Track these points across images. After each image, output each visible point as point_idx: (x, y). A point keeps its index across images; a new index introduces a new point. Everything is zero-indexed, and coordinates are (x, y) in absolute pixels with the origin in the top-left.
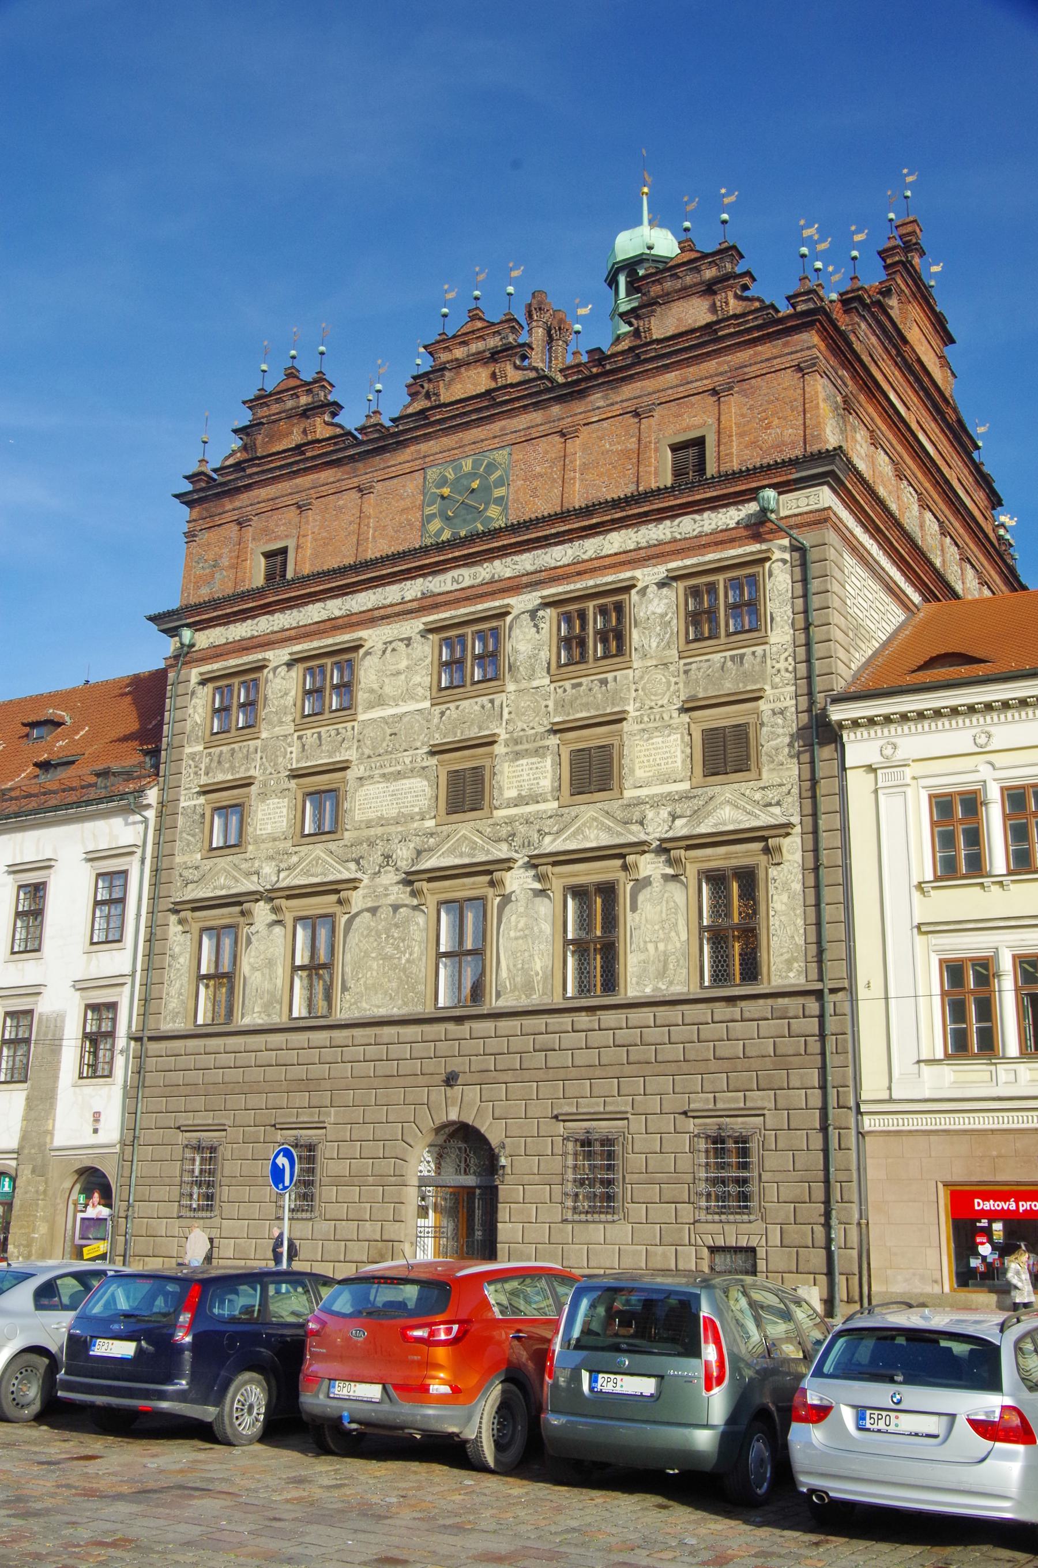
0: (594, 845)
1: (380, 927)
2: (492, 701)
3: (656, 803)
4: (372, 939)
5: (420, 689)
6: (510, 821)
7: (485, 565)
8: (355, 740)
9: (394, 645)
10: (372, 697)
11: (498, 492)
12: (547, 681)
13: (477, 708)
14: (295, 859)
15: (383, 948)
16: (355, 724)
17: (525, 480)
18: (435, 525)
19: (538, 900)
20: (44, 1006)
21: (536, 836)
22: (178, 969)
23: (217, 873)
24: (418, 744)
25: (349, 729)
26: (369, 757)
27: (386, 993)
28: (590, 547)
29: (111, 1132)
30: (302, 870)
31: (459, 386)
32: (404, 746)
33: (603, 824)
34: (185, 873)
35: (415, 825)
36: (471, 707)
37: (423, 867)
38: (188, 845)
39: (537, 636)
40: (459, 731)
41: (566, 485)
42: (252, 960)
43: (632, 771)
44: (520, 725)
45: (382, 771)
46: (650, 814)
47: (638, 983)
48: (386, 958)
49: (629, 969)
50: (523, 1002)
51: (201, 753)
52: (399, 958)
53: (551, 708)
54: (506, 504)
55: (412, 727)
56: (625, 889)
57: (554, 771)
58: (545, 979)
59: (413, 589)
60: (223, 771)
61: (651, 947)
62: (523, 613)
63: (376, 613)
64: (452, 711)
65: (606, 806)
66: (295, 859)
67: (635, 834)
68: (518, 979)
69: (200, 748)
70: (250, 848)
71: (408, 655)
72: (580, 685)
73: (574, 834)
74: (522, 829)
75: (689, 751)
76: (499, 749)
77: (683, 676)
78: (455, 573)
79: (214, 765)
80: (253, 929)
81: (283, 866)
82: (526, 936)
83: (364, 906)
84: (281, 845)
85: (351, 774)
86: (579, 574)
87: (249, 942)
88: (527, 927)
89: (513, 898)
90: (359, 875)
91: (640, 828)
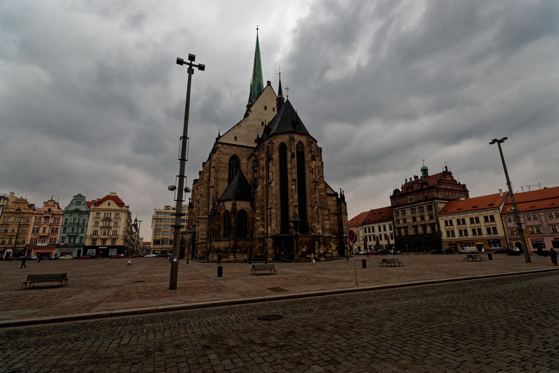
20: (388, 234)
28: (420, 204)
29: (394, 243)
36: (414, 214)
59: (408, 206)
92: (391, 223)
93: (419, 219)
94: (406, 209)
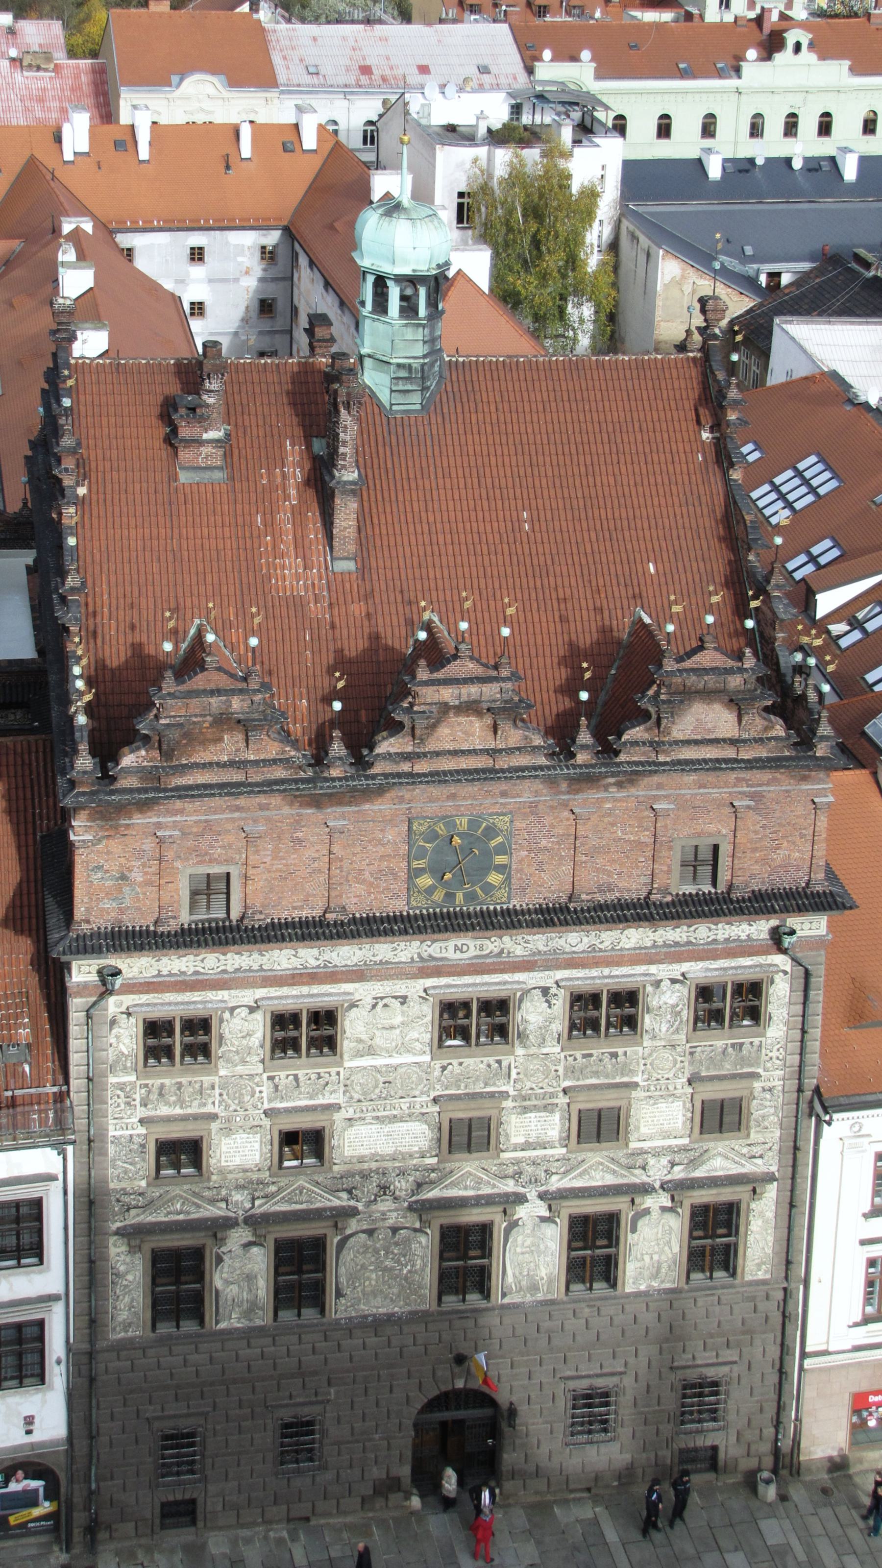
0: (600, 1183)
1: (378, 1245)
2: (499, 1062)
3: (657, 1153)
4: (369, 1255)
5: (417, 1043)
6: (517, 1162)
7: (493, 939)
8: (341, 1085)
9: (385, 1001)
10: (361, 1047)
11: (500, 859)
12: (558, 1049)
13: (483, 1066)
14: (273, 1188)
15: (382, 1262)
16: (341, 1070)
17: (529, 851)
18: (425, 881)
19: (544, 1225)
21: (543, 1174)
22: (126, 1286)
23: (171, 1200)
24: (417, 1093)
25: (333, 1073)
26: (359, 1101)
30: (283, 1198)
31: (447, 731)
32: (400, 1093)
33: (608, 1167)
34: (126, 1199)
35: (415, 1162)
39: (549, 1010)
40: (463, 1085)
41: (577, 868)
43: (638, 1128)
44: (529, 1085)
45: (375, 1114)
46: (652, 1161)
47: (634, 1283)
49: (628, 1273)
52: (401, 1270)
53: (561, 1072)
54: (509, 873)
55: (409, 1078)
56: (627, 1216)
57: (563, 1125)
58: (550, 1281)
61: (647, 1258)
62: (535, 988)
64: (455, 1068)
67: (638, 1177)
68: (524, 1283)
70: (214, 1178)
71: (403, 1013)
72: (591, 1055)
73: (580, 1175)
75: (689, 1115)
76: (508, 1104)
77: (688, 1057)
80: (224, 1249)
81: (257, 1194)
82: (532, 1251)
83: (359, 1228)
84: (255, 1177)
85: (339, 1117)
87: (219, 1260)
88: (533, 1244)
89: (520, 1223)
90: (352, 1203)
91: (641, 1171)
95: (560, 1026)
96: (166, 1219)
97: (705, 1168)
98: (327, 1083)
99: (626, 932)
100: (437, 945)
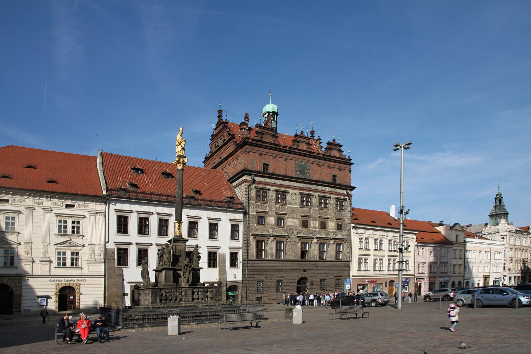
2: (309, 210)
3: (332, 232)
6: (312, 230)
10: (289, 202)
12: (317, 209)
13: (307, 210)
14: (276, 230)
19: (316, 244)
23: (260, 229)
27: (293, 256)
28: (324, 188)
32: (295, 213)
34: (253, 228)
36: (306, 209)
37: (299, 236)
38: (253, 222)
42: (268, 247)
43: (328, 226)
44: (313, 215)
46: (331, 234)
48: (293, 250)
50: (314, 259)
51: (254, 203)
59: (296, 184)
60: (259, 208)
63: (291, 187)
65: (325, 231)
66: (276, 230)
68: (313, 256)
69: (254, 202)
70: (267, 226)
71: (296, 197)
73: (321, 235)
74: (314, 232)
78: (304, 184)
79: (257, 206)
81: (273, 230)
82: (314, 249)
86: (323, 192)
87: (267, 244)
88: (315, 248)
92: (240, 216)
93: (314, 224)
94: (291, 191)
95: (318, 204)
96: (259, 233)
97: (338, 236)
98: (284, 209)
99: (327, 187)
100: (301, 184)
